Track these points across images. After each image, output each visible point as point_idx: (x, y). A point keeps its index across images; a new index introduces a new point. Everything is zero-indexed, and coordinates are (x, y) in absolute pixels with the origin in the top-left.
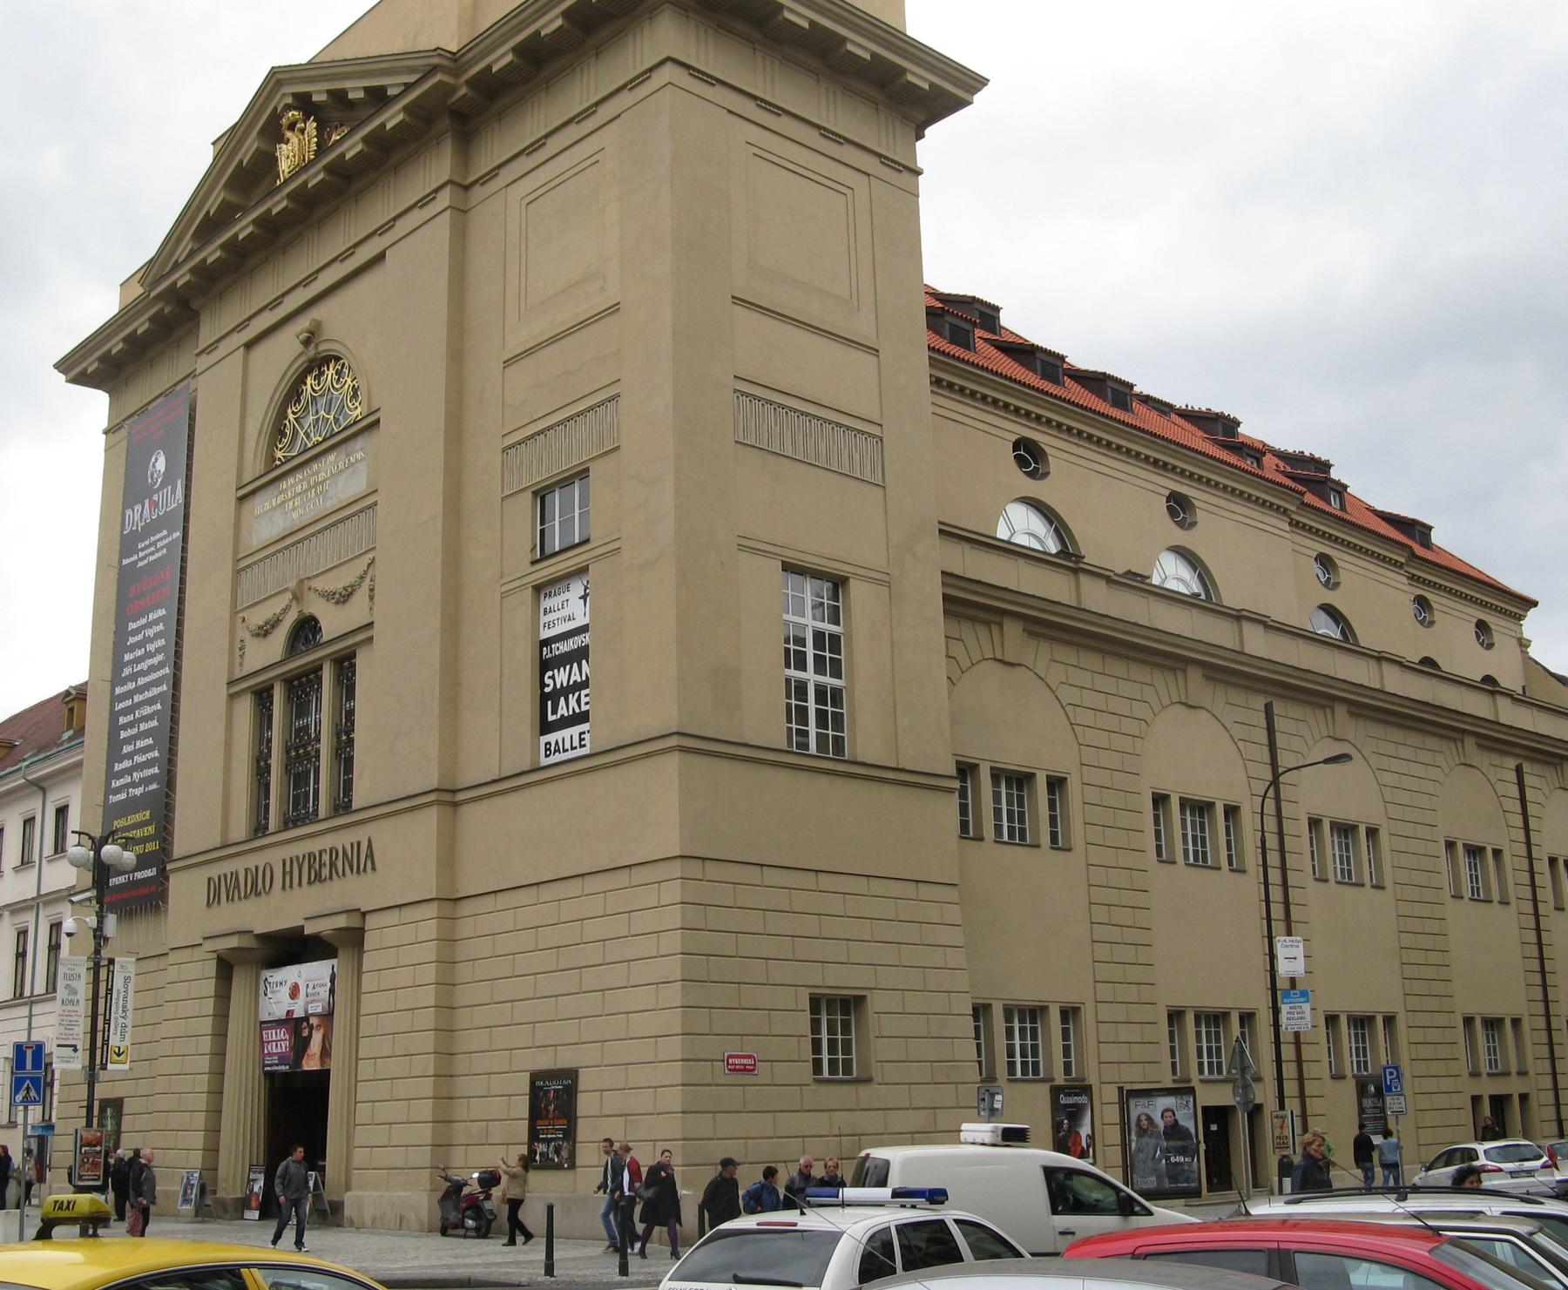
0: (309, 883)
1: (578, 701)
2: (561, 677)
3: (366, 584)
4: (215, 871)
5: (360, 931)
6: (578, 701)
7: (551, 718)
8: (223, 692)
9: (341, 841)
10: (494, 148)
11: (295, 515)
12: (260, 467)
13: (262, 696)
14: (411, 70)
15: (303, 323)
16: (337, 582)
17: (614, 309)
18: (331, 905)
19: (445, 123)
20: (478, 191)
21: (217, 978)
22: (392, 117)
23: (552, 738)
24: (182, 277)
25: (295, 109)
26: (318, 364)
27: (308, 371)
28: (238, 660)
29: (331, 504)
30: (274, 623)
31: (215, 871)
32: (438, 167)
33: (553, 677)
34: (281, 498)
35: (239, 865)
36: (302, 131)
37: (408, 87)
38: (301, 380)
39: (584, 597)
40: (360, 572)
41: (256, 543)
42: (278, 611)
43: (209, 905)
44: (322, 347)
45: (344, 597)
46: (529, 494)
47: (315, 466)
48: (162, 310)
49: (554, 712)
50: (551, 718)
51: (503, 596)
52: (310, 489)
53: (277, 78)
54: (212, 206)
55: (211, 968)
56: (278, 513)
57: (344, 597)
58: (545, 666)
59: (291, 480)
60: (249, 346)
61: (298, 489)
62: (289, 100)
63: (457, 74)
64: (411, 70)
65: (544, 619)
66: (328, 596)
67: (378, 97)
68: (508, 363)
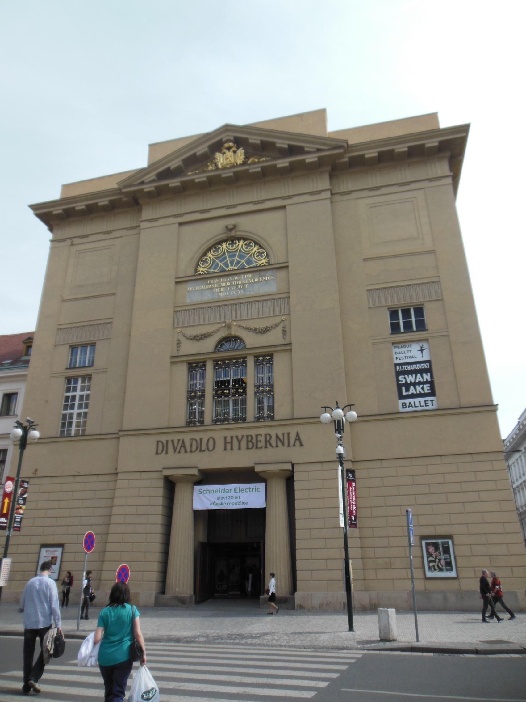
0: (248, 448)
1: (423, 388)
2: (410, 379)
3: (279, 329)
4: (163, 438)
5: (293, 471)
6: (423, 388)
7: (404, 393)
8: (169, 360)
9: (273, 432)
10: (348, 184)
11: (221, 294)
12: (190, 272)
13: (195, 366)
14: (324, 144)
15: (231, 222)
17: (433, 252)
18: (264, 459)
19: (329, 168)
20: (337, 198)
21: (164, 488)
22: (311, 159)
23: (407, 401)
24: (148, 188)
25: (231, 141)
26: (233, 240)
27: (225, 241)
29: (248, 294)
30: (205, 336)
31: (163, 438)
32: (323, 183)
33: (405, 378)
34: (207, 287)
35: (187, 438)
36: (235, 152)
37: (319, 150)
38: (220, 243)
39: (422, 350)
41: (188, 301)
43: (157, 453)
44: (238, 233)
45: (264, 331)
46: (387, 308)
47: (236, 278)
48: (121, 199)
49: (407, 390)
50: (404, 393)
51: (374, 344)
52: (233, 286)
53: (227, 128)
54: (174, 165)
55: (161, 483)
57: (264, 331)
58: (398, 374)
59: (216, 281)
60: (181, 224)
61: (224, 284)
62: (232, 138)
63: (346, 152)
64: (324, 144)
65: (395, 356)
66: (255, 330)
67: (292, 150)
68: (365, 260)
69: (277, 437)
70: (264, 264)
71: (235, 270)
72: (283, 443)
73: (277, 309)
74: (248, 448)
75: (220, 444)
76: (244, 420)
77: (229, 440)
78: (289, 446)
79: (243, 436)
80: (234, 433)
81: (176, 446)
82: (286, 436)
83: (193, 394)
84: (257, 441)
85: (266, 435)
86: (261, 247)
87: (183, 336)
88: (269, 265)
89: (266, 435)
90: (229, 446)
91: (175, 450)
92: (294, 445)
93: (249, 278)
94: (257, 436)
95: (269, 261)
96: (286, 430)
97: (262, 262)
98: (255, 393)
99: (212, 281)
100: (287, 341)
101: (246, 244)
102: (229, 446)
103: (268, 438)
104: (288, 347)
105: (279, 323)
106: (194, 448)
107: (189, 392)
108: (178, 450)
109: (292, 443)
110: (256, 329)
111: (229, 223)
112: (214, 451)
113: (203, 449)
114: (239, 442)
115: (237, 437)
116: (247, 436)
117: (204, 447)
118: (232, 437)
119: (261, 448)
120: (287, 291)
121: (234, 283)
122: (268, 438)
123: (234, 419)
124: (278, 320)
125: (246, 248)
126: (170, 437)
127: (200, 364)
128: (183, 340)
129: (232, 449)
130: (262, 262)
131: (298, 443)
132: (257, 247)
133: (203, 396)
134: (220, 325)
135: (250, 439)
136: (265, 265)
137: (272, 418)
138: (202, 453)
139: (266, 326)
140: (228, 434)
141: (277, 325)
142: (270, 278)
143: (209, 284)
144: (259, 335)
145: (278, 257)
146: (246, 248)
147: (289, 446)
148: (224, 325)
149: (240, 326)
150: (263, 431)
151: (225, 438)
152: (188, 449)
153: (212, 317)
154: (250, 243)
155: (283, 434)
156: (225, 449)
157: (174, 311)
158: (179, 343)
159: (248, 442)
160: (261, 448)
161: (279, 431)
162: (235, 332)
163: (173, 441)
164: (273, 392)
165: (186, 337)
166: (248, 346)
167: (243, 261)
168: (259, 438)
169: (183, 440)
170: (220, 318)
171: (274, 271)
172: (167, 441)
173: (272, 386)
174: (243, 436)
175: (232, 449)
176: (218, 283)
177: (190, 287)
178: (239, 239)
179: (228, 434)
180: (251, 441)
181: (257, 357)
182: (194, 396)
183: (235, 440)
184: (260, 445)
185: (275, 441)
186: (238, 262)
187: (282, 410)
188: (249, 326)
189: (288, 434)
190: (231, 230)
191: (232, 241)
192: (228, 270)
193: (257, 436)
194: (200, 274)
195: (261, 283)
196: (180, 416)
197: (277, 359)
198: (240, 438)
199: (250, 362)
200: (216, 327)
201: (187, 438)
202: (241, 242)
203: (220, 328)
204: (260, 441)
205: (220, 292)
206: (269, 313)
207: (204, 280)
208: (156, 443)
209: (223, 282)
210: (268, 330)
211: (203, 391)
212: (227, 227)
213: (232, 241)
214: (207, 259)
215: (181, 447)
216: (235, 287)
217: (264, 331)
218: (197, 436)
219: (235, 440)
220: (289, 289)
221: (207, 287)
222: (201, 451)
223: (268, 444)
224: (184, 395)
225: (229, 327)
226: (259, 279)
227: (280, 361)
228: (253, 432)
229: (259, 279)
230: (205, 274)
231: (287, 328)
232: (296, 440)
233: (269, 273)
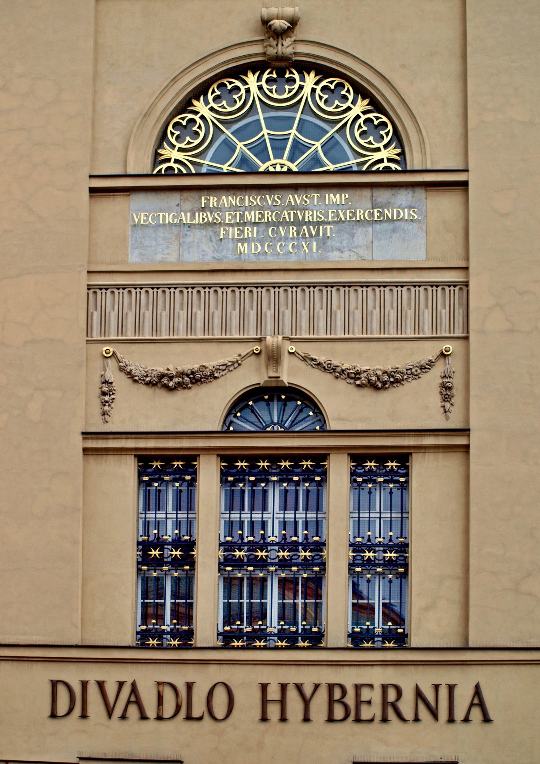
0: (331, 719)
3: (433, 379)
8: (79, 443)
9: (407, 680)
11: (243, 248)
13: (164, 468)
16: (374, 360)
27: (258, 67)
28: (96, 408)
29: (335, 258)
30: (196, 379)
34: (199, 218)
35: (146, 679)
38: (238, 72)
40: (424, 359)
42: (211, 364)
44: (302, 49)
52: (286, 224)
56: (198, 234)
59: (227, 200)
61: (252, 216)
69: (419, 694)
70: (386, 164)
71: (290, 172)
72: (435, 714)
73: (427, 316)
74: (331, 719)
75: (248, 701)
76: (316, 640)
77: (274, 693)
78: (451, 720)
79: (317, 687)
80: (292, 676)
81: (111, 700)
82: (443, 693)
83: (155, 553)
84: (358, 702)
85: (384, 688)
86: (376, 106)
87: (122, 369)
88: (405, 172)
89: (384, 688)
90: (274, 711)
91: (110, 714)
92: (466, 720)
93: (335, 205)
94: (358, 688)
95: (402, 154)
96: (445, 677)
97: (377, 156)
98: (352, 565)
99: (213, 201)
100: (455, 423)
101: (324, 89)
102: (274, 711)
103: (392, 696)
104: (460, 441)
105: (431, 363)
106: (169, 709)
107: (144, 547)
108: (118, 711)
109: (459, 715)
110: (358, 373)
111: (274, 10)
112: (230, 720)
113: (196, 713)
114: (306, 702)
115: (299, 687)
116: (331, 687)
117: (198, 709)
118: (284, 687)
119: (371, 720)
120: (462, 264)
121: (287, 215)
122: (392, 696)
123: (281, 635)
124: (429, 351)
125: (363, 134)
126: (92, 674)
127: (177, 464)
128: (120, 382)
129: (283, 719)
130: (377, 156)
131: (476, 714)
132: (361, 105)
133: (188, 560)
134: (244, 349)
135: (337, 694)
136: (387, 171)
137: (401, 640)
138: (195, 725)
139: (389, 368)
140: (274, 677)
141: (425, 368)
142: (405, 214)
143: (203, 209)
144: (368, 392)
145: (432, 152)
146: (363, 134)
147: (451, 720)
148: (256, 347)
149: (305, 359)
150: (378, 676)
151: (264, 687)
152: (151, 712)
153: (217, 321)
154: (340, 86)
155: (436, 687)
156: (264, 719)
157: (89, 288)
158: (107, 391)
159: (331, 701)
160: (371, 720)
161: (425, 678)
162: (291, 374)
163: (101, 685)
164: (406, 566)
165: (129, 373)
166: (333, 425)
167: (318, 145)
168: (365, 694)
169: (134, 686)
170: (242, 327)
171: (420, 193)
172: (84, 685)
173: (403, 548)
174: (317, 687)
175: (283, 719)
176: (236, 208)
177: (141, 210)
178: (304, 67)
179: (274, 677)
180: (339, 701)
181: (358, 458)
182: (163, 562)
183: (292, 695)
184: (366, 713)
185: (412, 705)
186: (298, 148)
187: (429, 624)
188: (335, 362)
189: (451, 688)
190: (280, 35)
191: (281, 73)
192: (267, 173)
193: (358, 688)
194: (170, 173)
195: (378, 227)
196: (120, 615)
197: (421, 468)
198: (308, 690)
199: (339, 470)
200: (230, 353)
201: (146, 679)
202: (311, 79)
203: (244, 358)
204: (369, 702)
205: (243, 241)
206: (399, 327)
207: (186, 194)
208: (48, 688)
209: (251, 208)
210: (397, 381)
211: (188, 547)
212: (265, 22)
213: (281, 73)
214: (192, 121)
215: (129, 702)
216: (292, 230)
217: (384, 383)
218: (179, 677)
219: (292, 695)
220: (467, 259)
221: (199, 218)
222: (189, 718)
223: (391, 713)
224: (131, 555)
225: (274, 358)
226: (371, 214)
227: (429, 476)
228: (348, 678)
229: (371, 214)
230: (190, 175)
231: (457, 382)
232: (472, 705)
233: (404, 197)
